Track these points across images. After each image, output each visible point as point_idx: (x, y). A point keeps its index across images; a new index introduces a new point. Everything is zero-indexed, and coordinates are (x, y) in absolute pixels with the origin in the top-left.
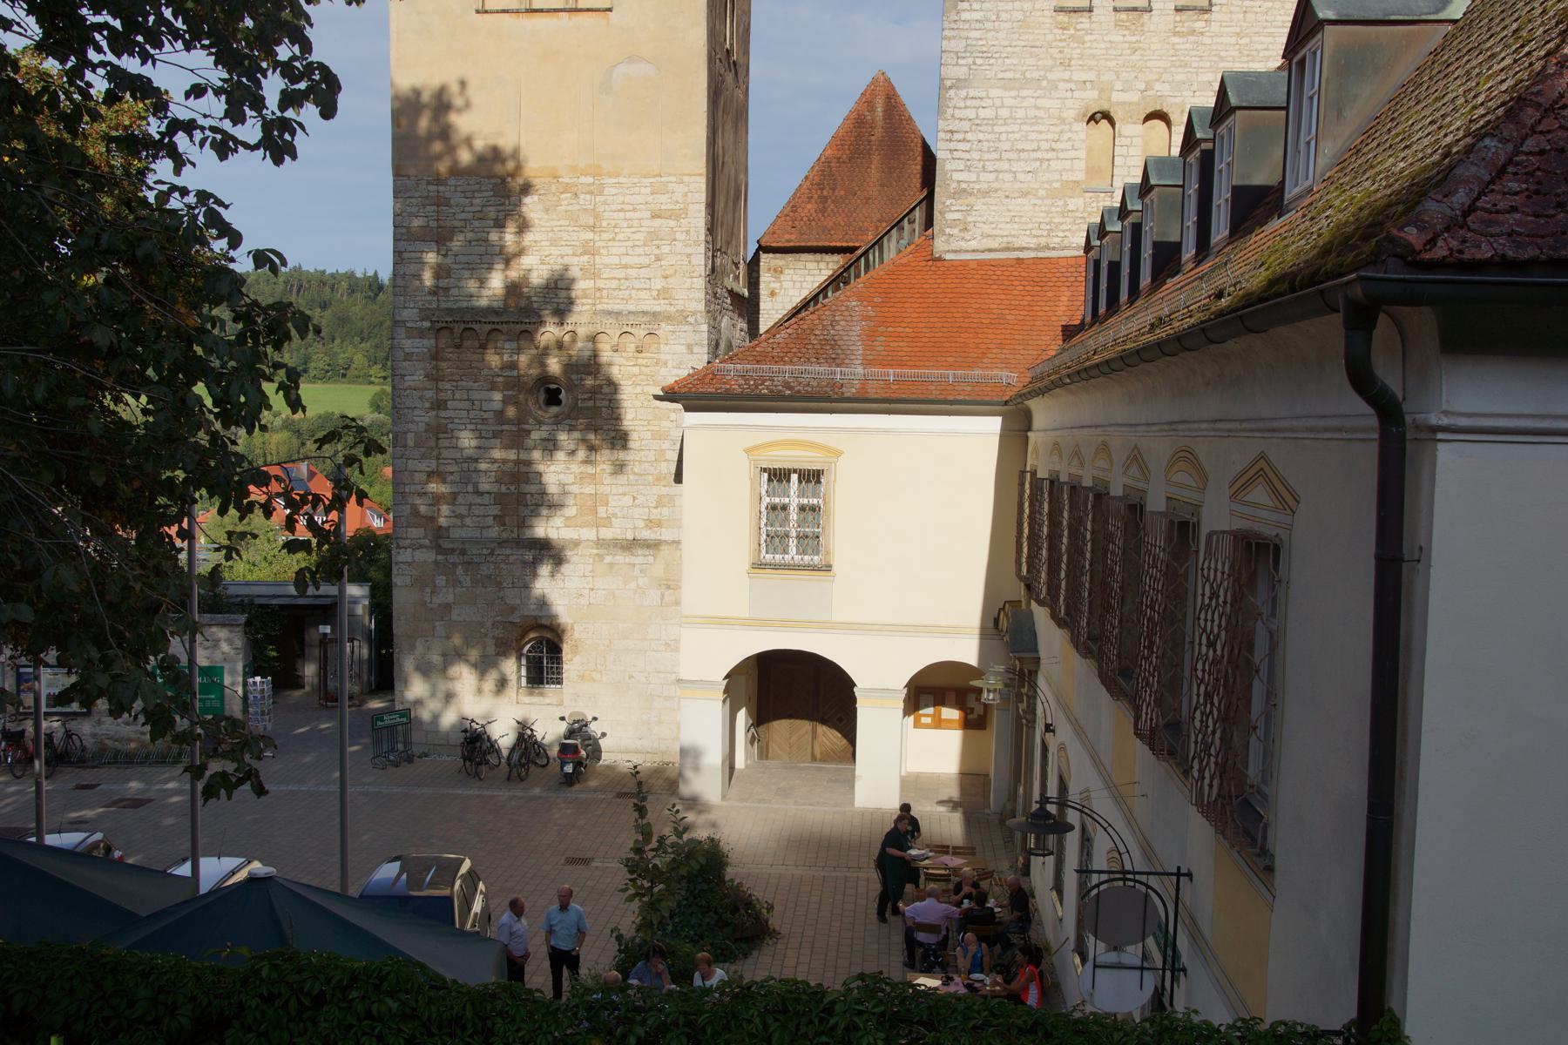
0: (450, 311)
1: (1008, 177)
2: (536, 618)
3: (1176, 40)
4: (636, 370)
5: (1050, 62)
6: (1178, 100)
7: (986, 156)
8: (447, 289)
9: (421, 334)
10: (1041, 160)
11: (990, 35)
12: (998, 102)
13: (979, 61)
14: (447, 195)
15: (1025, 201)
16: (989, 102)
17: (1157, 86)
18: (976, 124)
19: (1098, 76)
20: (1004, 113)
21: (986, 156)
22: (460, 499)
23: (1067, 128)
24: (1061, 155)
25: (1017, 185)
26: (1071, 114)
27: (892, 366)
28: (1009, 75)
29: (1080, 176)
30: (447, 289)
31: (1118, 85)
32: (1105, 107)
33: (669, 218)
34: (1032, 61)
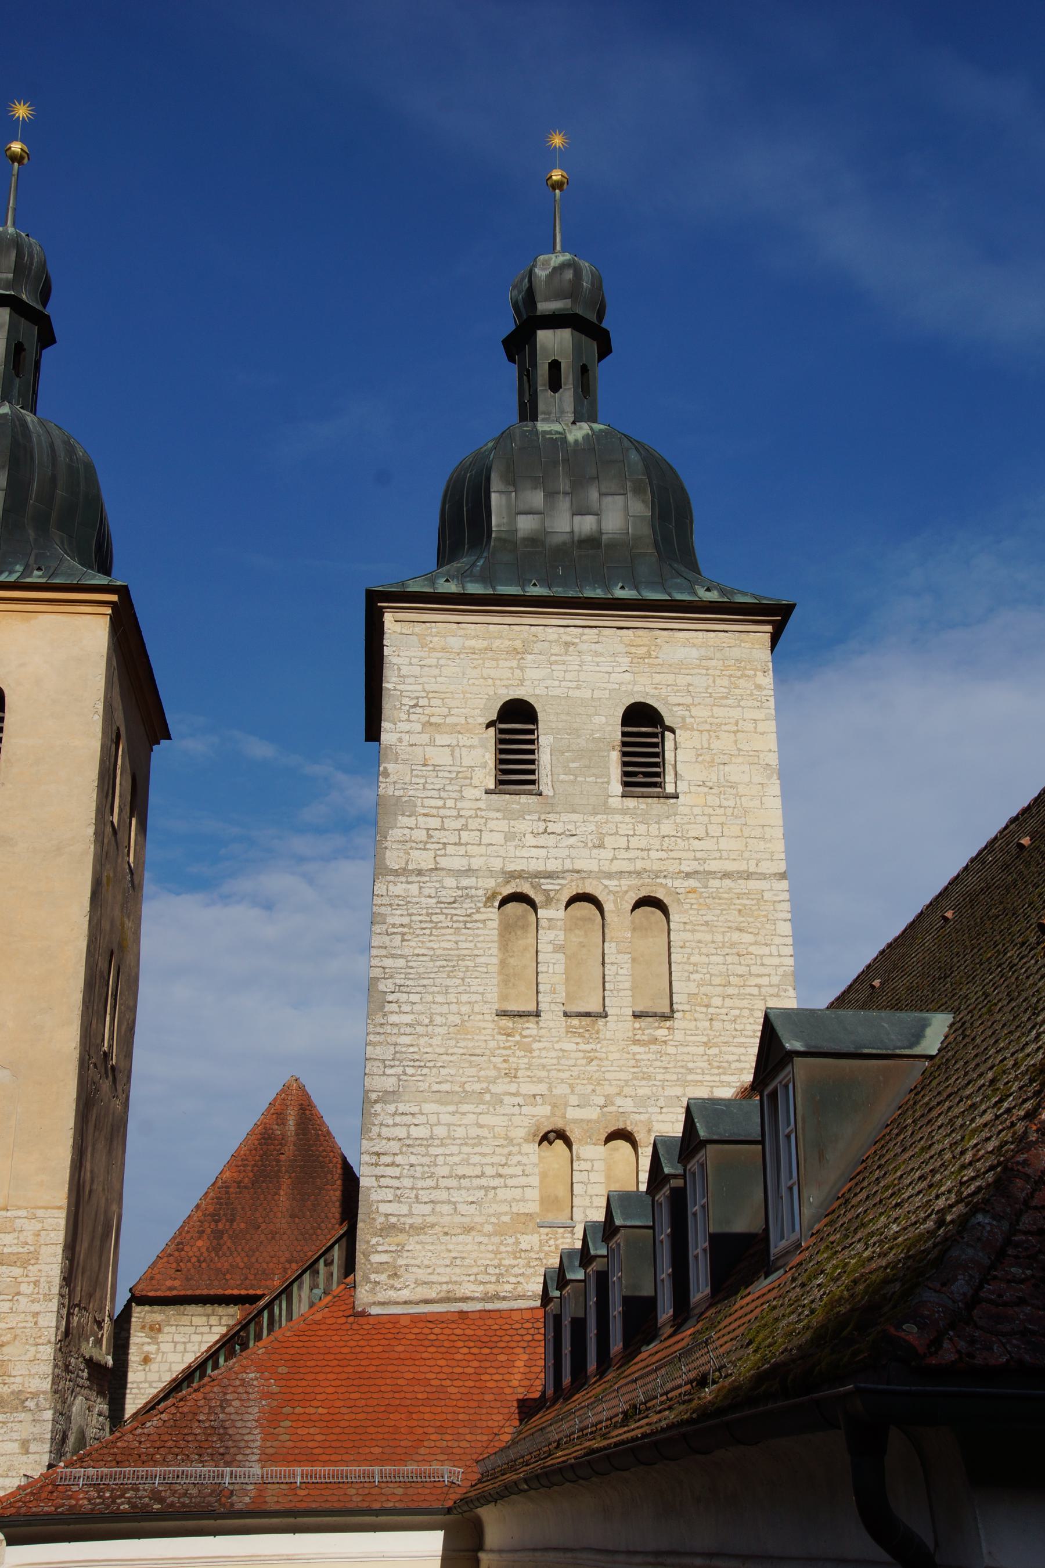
1: (446, 1208)
3: (636, 1049)
5: (493, 1073)
6: (643, 1117)
7: (420, 1184)
10: (486, 1189)
11: (423, 1041)
12: (433, 1119)
13: (410, 1071)
15: (468, 1238)
16: (421, 1119)
17: (619, 1101)
18: (407, 1144)
19: (550, 1089)
20: (440, 1131)
21: (420, 1184)
23: (515, 1149)
24: (510, 1182)
25: (458, 1219)
26: (521, 1133)
27: (299, 1462)
28: (445, 1087)
29: (533, 1207)
31: (574, 1100)
32: (560, 1124)
33: (14, 1264)
34: (473, 1071)
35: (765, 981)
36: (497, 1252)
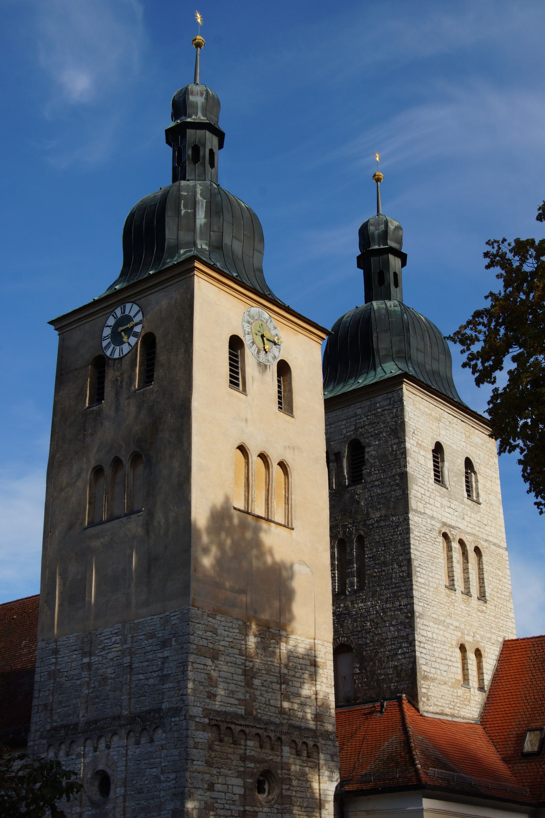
0: (218, 712)
9: (204, 728)
14: (216, 626)
16: (429, 629)
20: (435, 636)
35: (505, 593)
36: (453, 695)
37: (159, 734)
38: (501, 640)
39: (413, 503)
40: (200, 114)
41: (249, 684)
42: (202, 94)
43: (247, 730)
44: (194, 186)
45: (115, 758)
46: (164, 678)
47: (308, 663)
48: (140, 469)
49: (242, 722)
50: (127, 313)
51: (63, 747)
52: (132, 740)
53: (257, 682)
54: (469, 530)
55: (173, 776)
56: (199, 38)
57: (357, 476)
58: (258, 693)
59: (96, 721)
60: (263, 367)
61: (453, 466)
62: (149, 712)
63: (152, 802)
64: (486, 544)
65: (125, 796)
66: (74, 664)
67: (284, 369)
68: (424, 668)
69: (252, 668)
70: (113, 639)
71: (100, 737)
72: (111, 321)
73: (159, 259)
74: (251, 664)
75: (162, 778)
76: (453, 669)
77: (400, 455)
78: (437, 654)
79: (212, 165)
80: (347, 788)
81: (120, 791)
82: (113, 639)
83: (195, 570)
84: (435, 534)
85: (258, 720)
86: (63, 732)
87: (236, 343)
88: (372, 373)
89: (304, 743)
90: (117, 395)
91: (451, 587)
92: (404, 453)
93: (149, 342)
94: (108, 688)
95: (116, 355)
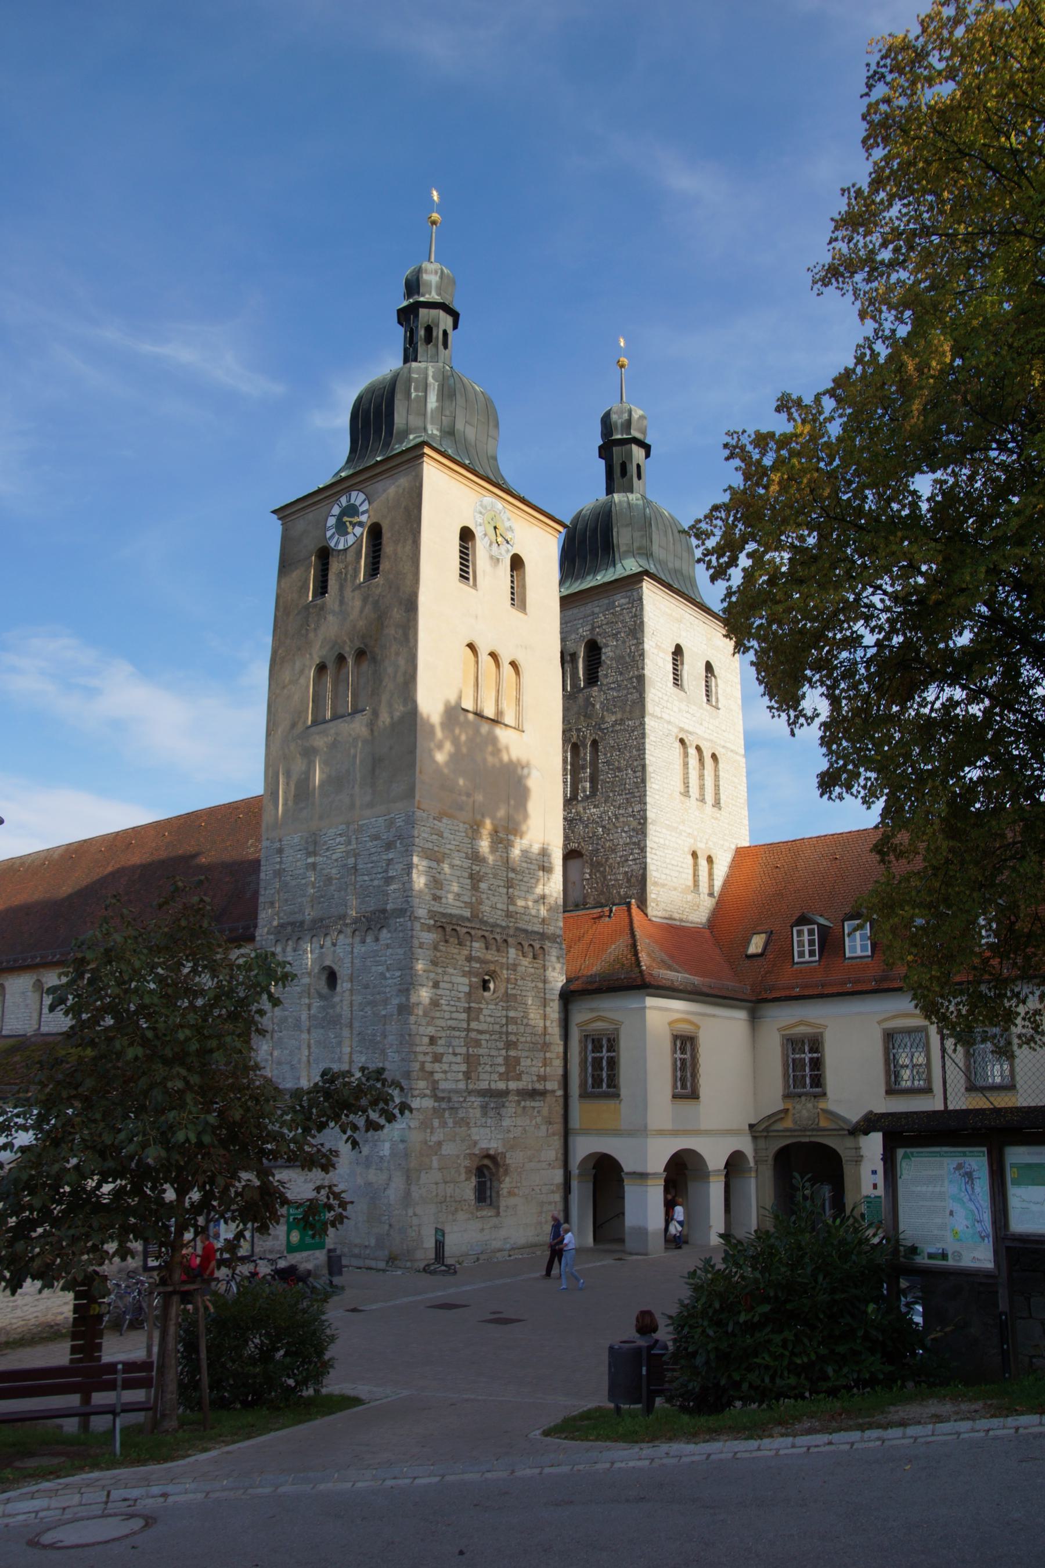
0: (444, 915)
2: (488, 1149)
4: (532, 970)
8: (440, 898)
9: (429, 929)
14: (442, 829)
20: (667, 842)
22: (444, 1059)
30: (440, 898)
37: (384, 934)
38: (733, 847)
39: (650, 707)
40: (434, 293)
41: (475, 888)
42: (436, 273)
43: (473, 932)
44: (427, 368)
45: (341, 955)
46: (389, 880)
47: (536, 867)
48: (365, 666)
49: (468, 925)
50: (352, 502)
51: (290, 943)
52: (357, 939)
53: (483, 886)
54: (706, 736)
55: (398, 973)
56: (435, 216)
57: (592, 678)
58: (484, 896)
59: (322, 920)
60: (496, 561)
61: (693, 670)
62: (374, 913)
63: (378, 997)
64: (722, 751)
65: (351, 990)
66: (298, 864)
67: (517, 563)
68: (654, 874)
69: (478, 872)
70: (338, 840)
71: (326, 935)
72: (336, 510)
73: (387, 445)
74: (478, 868)
75: (388, 975)
76: (684, 876)
77: (636, 658)
78: (668, 861)
79: (445, 345)
80: (572, 987)
81: (347, 985)
82: (338, 840)
83: (421, 772)
84: (672, 739)
85: (485, 923)
86: (289, 928)
87: (466, 535)
88: (611, 570)
89: (531, 945)
90: (341, 588)
91: (686, 793)
92: (642, 655)
93: (375, 532)
94: (333, 888)
95: (341, 547)
